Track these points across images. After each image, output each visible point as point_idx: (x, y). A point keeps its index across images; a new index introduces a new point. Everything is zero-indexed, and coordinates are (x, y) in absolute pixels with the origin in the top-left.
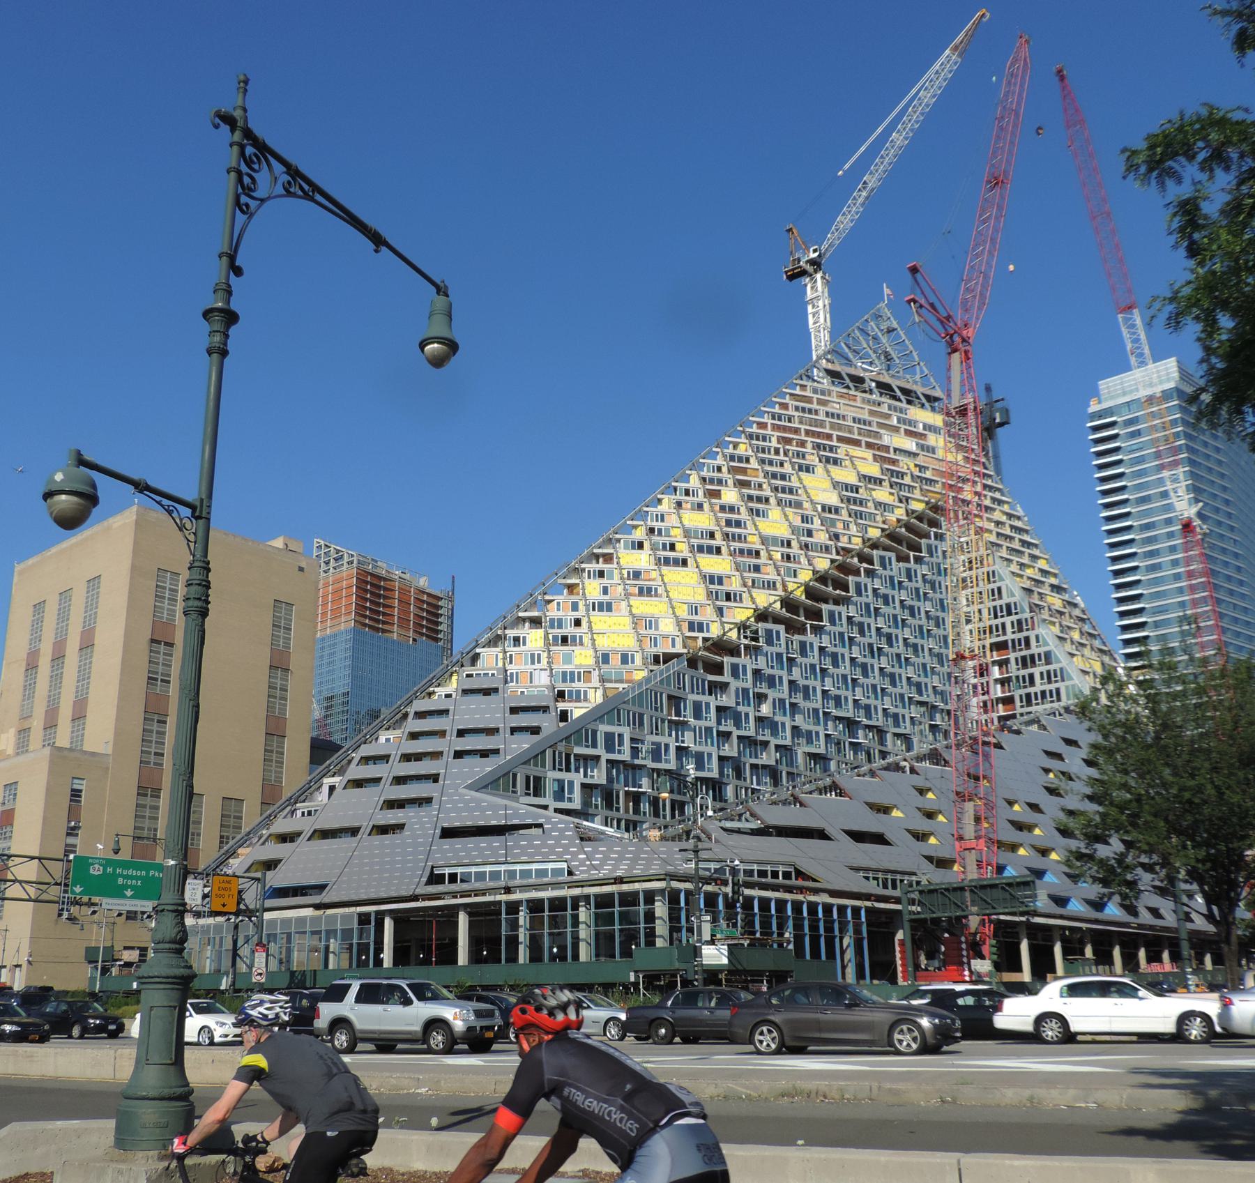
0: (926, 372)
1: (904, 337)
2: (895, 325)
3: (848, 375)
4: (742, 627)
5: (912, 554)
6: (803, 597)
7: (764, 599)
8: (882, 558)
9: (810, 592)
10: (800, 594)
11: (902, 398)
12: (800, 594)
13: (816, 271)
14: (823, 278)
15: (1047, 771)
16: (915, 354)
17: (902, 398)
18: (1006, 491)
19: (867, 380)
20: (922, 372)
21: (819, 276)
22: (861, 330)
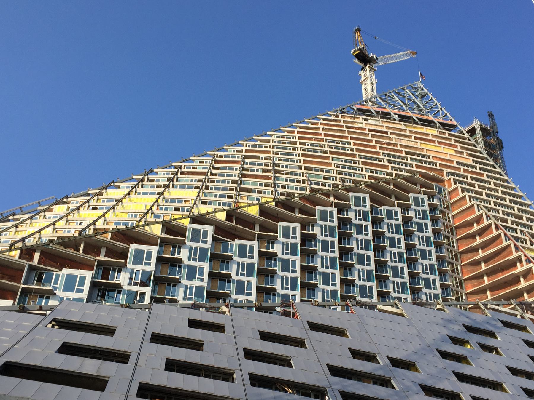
0: (445, 112)
1: (431, 96)
2: (426, 91)
3: (375, 111)
4: (168, 227)
5: (396, 201)
6: (258, 215)
7: (204, 209)
8: (357, 199)
9: (263, 211)
10: (254, 211)
11: (419, 123)
12: (254, 211)
13: (366, 65)
14: (371, 69)
15: (461, 342)
16: (438, 104)
17: (419, 123)
18: (503, 173)
19: (392, 114)
20: (443, 113)
21: (367, 68)
22: (397, 93)
